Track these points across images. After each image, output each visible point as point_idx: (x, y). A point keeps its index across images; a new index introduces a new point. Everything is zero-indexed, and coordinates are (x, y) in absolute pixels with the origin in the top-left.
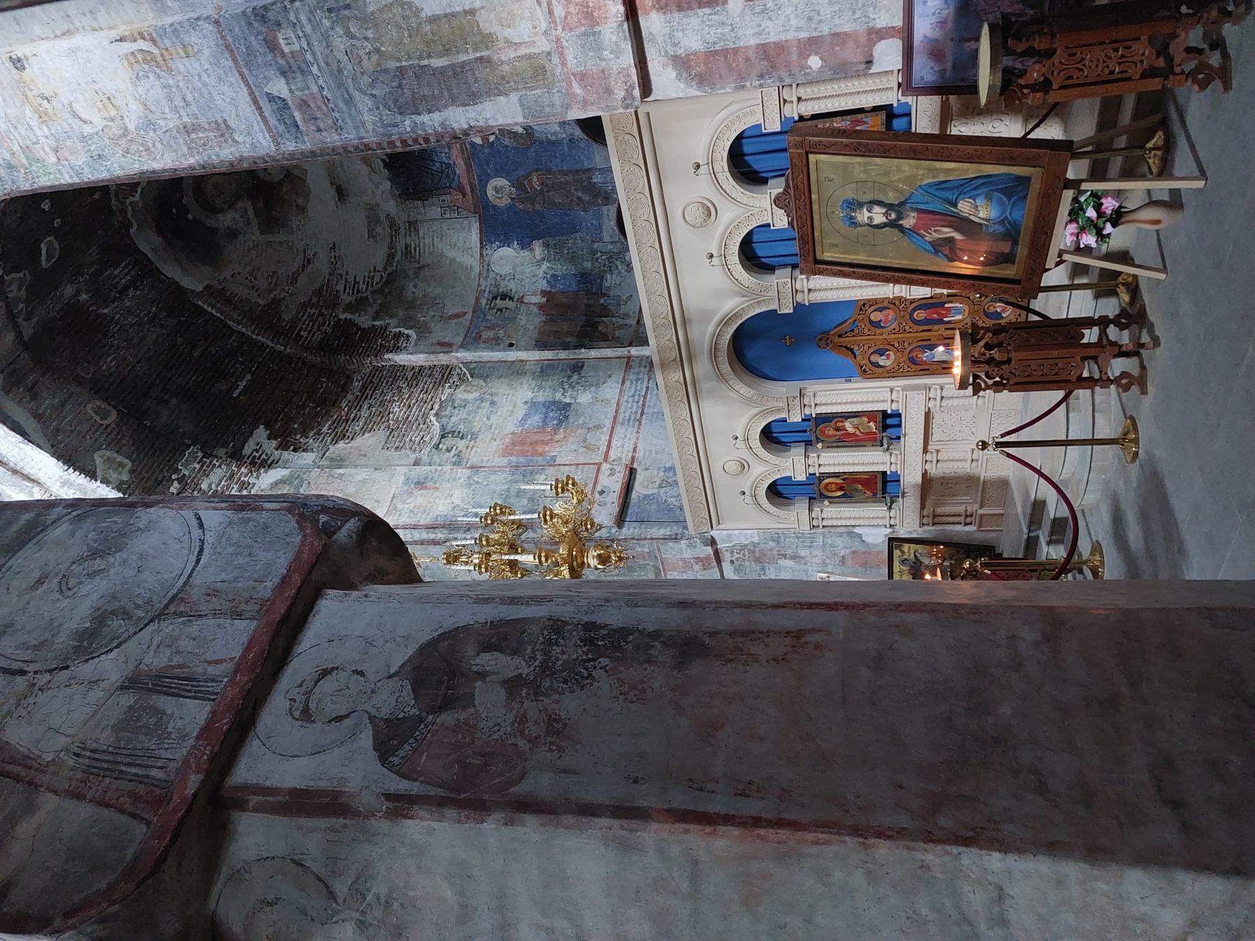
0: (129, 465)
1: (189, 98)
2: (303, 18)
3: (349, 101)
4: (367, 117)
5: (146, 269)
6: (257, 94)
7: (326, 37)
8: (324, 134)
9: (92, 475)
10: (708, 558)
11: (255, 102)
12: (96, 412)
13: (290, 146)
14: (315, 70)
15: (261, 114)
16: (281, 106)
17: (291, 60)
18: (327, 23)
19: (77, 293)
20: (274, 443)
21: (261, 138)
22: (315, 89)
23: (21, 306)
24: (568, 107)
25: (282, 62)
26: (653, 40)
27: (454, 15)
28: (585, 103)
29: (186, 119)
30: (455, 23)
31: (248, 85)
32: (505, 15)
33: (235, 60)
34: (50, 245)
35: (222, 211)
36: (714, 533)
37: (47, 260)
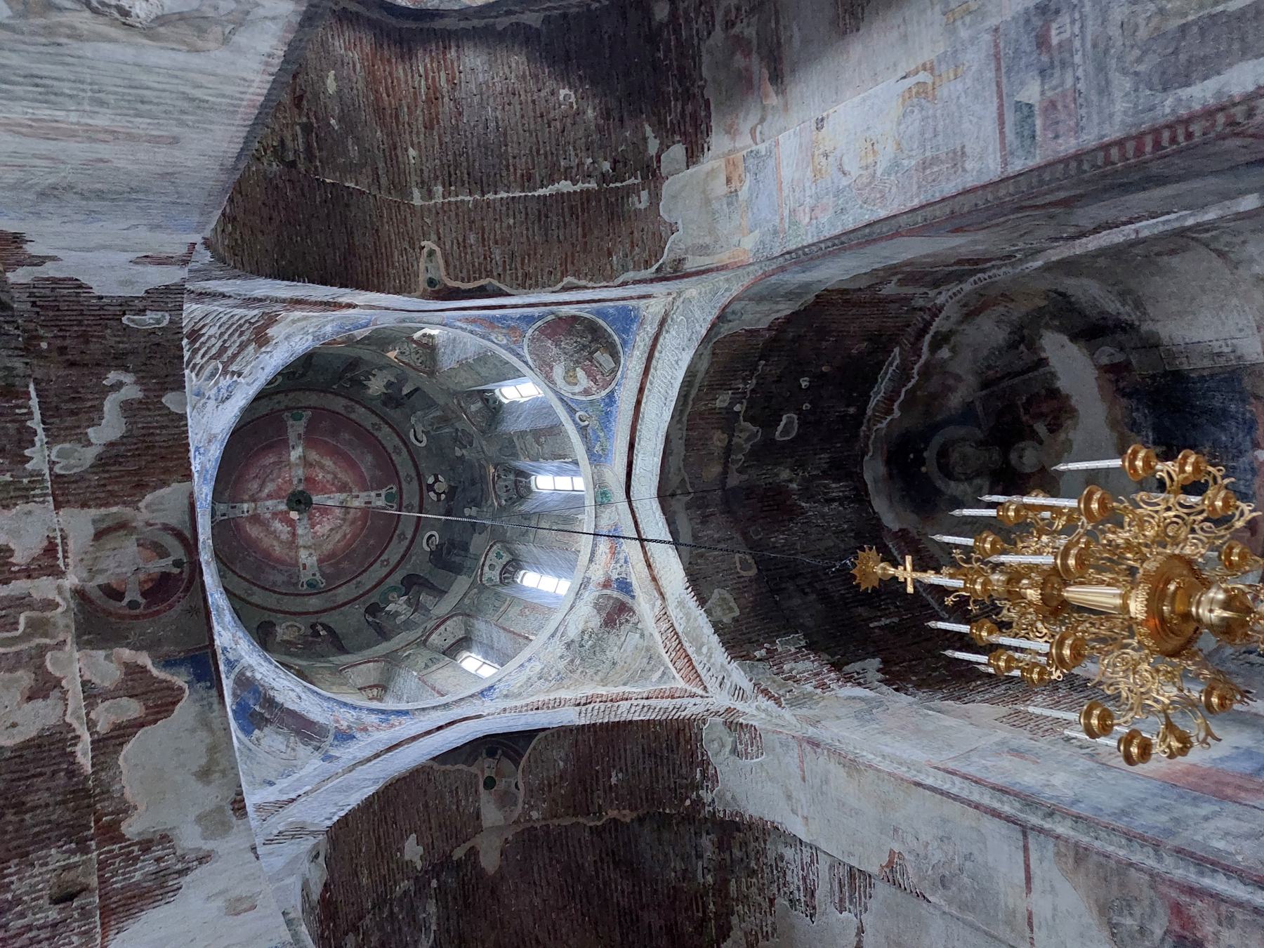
0: (737, 613)
1: (940, 128)
5: (860, 496)
6: (1006, 105)
8: (1060, 141)
9: (702, 601)
11: (1001, 116)
12: (742, 564)
13: (1018, 165)
15: (1002, 132)
16: (1025, 111)
19: (791, 481)
20: (880, 676)
21: (990, 161)
23: (740, 456)
31: (1000, 97)
33: (998, 69)
34: (790, 422)
35: (958, 480)
37: (781, 435)
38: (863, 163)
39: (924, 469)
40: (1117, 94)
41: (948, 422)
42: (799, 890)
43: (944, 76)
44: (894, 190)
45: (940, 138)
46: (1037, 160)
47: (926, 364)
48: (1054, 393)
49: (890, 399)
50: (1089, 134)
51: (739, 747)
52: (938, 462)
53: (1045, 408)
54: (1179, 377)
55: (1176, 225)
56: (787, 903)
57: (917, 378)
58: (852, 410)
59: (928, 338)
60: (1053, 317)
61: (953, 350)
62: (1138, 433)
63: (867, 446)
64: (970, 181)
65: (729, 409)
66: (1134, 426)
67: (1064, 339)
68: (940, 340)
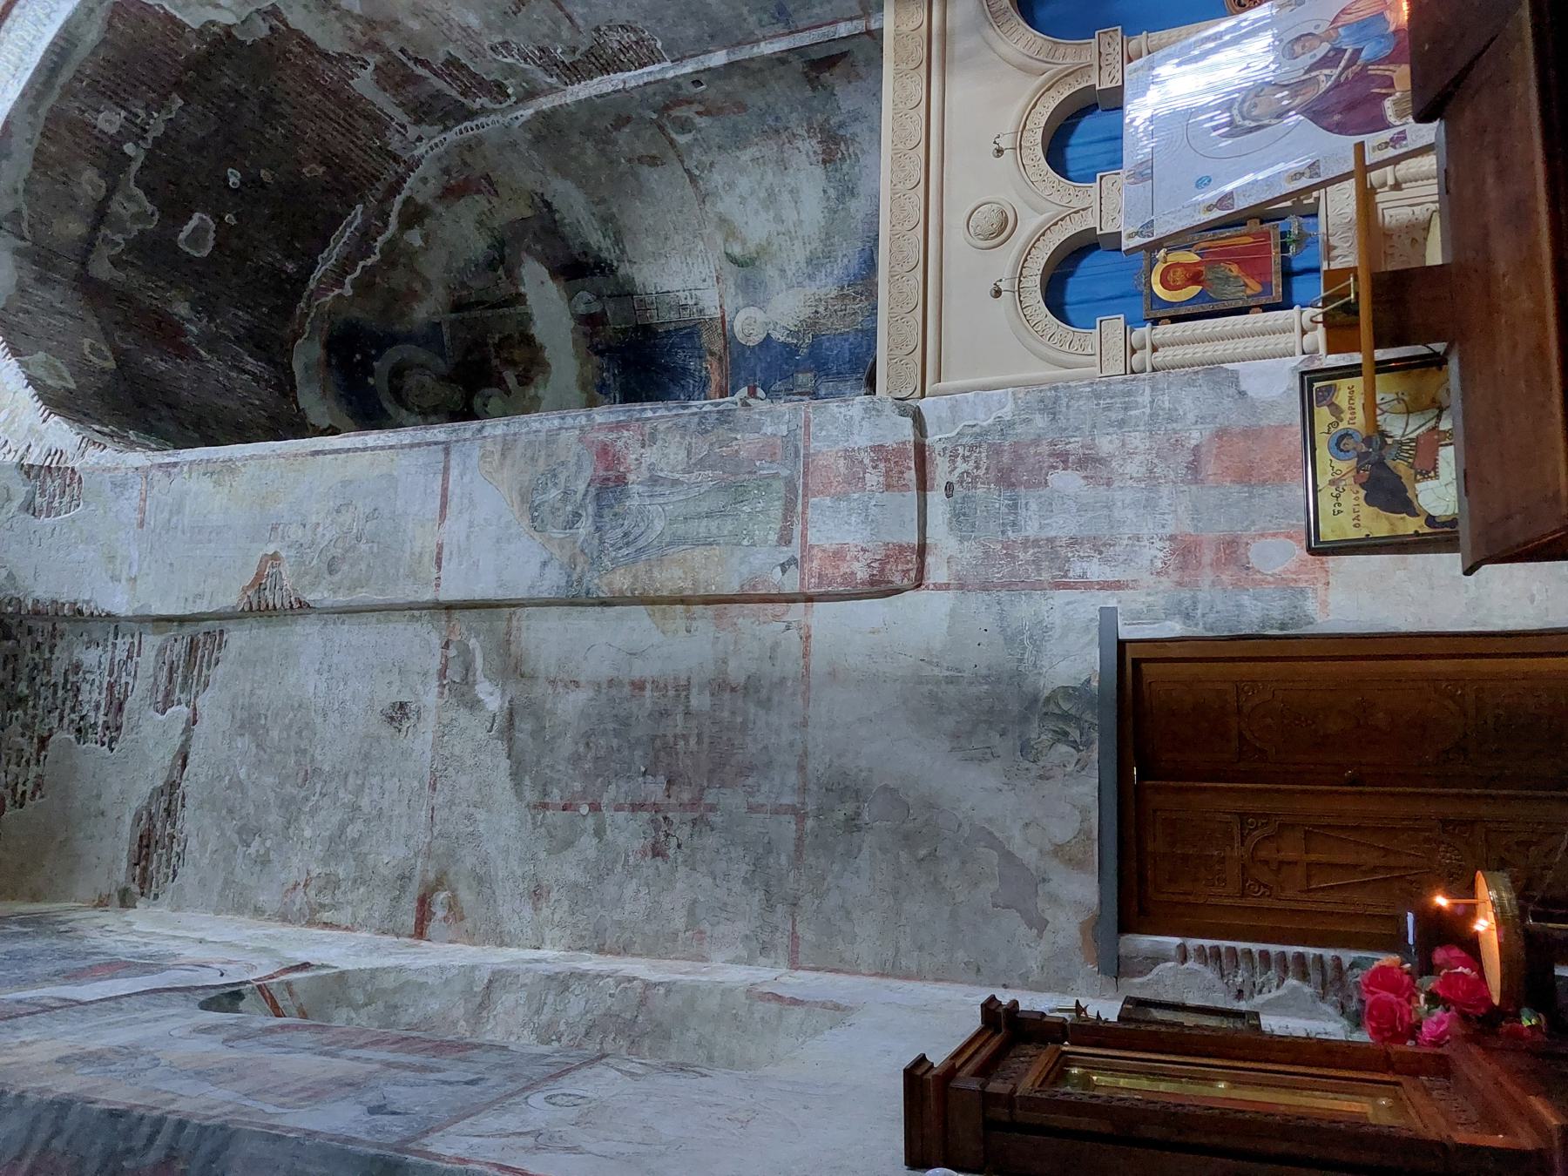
10: (900, 452)
23: (119, 238)
36: (925, 405)
39: (371, 381)
42: (97, 707)
47: (389, 242)
48: (528, 340)
51: (38, 500)
52: (390, 381)
53: (517, 354)
54: (648, 330)
55: (659, 77)
56: (72, 737)
57: (378, 257)
58: (290, 267)
59: (399, 199)
60: (537, 239)
61: (425, 238)
63: (302, 325)
65: (117, 141)
67: (544, 272)
68: (414, 215)
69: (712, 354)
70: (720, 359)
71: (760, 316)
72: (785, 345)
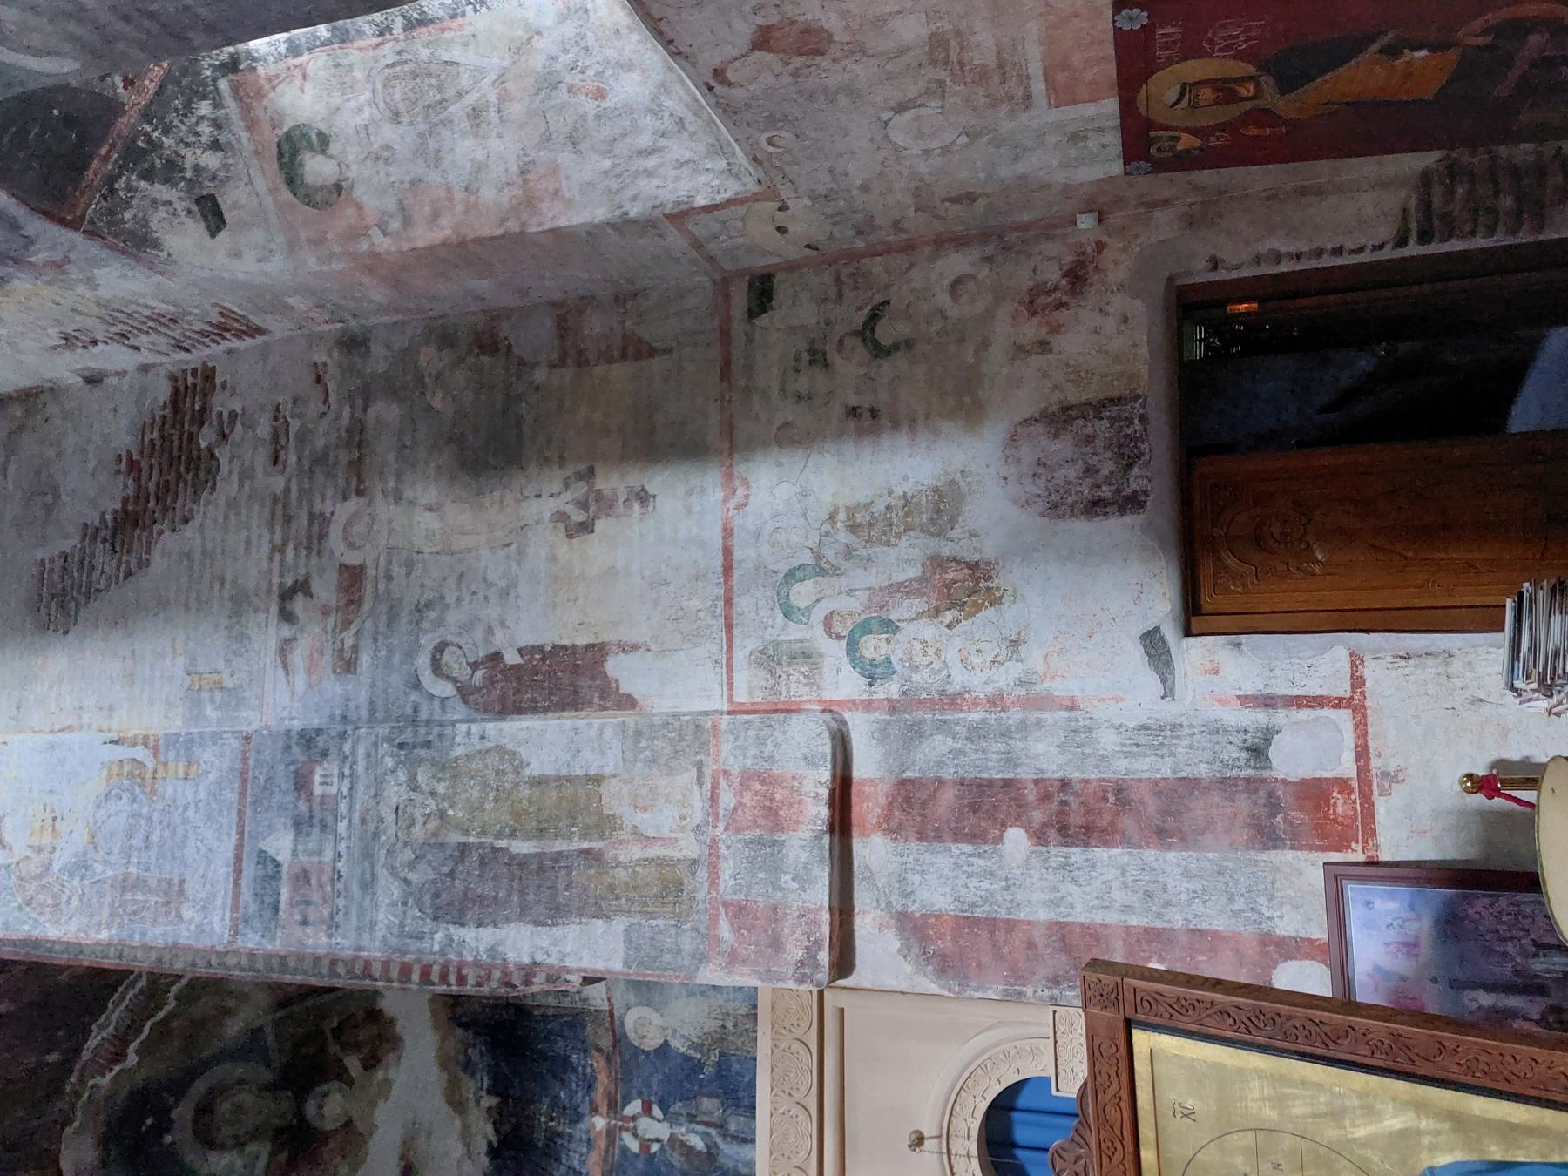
1: (155, 838)
2: (361, 751)
3: (368, 885)
4: (384, 917)
6: (247, 848)
7: (379, 782)
8: (309, 930)
11: (238, 859)
13: (251, 941)
14: (342, 827)
15: (236, 884)
16: (270, 868)
17: (316, 808)
18: (389, 762)
21: (217, 919)
22: (328, 856)
24: (701, 959)
25: (303, 807)
26: (870, 879)
27: (570, 780)
28: (733, 959)
29: (133, 869)
30: (568, 791)
31: (241, 833)
32: (644, 792)
33: (242, 794)
35: (222, 1147)
38: (35, 841)
39: (168, 1139)
40: (383, 900)
41: (218, 1059)
43: (171, 766)
44: (75, 902)
45: (153, 853)
46: (277, 945)
49: (121, 1041)
50: (344, 937)
52: (195, 1122)
62: (472, 1075)
63: (73, 1106)
64: (185, 936)
66: (468, 1067)
69: (599, 1050)
70: (609, 1059)
71: (657, 1020)
72: (686, 1058)
